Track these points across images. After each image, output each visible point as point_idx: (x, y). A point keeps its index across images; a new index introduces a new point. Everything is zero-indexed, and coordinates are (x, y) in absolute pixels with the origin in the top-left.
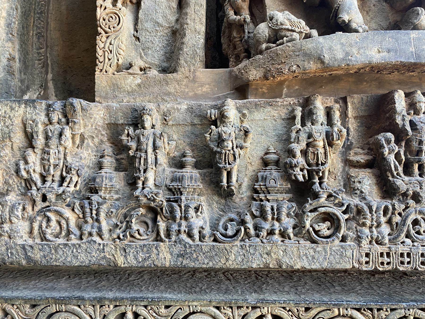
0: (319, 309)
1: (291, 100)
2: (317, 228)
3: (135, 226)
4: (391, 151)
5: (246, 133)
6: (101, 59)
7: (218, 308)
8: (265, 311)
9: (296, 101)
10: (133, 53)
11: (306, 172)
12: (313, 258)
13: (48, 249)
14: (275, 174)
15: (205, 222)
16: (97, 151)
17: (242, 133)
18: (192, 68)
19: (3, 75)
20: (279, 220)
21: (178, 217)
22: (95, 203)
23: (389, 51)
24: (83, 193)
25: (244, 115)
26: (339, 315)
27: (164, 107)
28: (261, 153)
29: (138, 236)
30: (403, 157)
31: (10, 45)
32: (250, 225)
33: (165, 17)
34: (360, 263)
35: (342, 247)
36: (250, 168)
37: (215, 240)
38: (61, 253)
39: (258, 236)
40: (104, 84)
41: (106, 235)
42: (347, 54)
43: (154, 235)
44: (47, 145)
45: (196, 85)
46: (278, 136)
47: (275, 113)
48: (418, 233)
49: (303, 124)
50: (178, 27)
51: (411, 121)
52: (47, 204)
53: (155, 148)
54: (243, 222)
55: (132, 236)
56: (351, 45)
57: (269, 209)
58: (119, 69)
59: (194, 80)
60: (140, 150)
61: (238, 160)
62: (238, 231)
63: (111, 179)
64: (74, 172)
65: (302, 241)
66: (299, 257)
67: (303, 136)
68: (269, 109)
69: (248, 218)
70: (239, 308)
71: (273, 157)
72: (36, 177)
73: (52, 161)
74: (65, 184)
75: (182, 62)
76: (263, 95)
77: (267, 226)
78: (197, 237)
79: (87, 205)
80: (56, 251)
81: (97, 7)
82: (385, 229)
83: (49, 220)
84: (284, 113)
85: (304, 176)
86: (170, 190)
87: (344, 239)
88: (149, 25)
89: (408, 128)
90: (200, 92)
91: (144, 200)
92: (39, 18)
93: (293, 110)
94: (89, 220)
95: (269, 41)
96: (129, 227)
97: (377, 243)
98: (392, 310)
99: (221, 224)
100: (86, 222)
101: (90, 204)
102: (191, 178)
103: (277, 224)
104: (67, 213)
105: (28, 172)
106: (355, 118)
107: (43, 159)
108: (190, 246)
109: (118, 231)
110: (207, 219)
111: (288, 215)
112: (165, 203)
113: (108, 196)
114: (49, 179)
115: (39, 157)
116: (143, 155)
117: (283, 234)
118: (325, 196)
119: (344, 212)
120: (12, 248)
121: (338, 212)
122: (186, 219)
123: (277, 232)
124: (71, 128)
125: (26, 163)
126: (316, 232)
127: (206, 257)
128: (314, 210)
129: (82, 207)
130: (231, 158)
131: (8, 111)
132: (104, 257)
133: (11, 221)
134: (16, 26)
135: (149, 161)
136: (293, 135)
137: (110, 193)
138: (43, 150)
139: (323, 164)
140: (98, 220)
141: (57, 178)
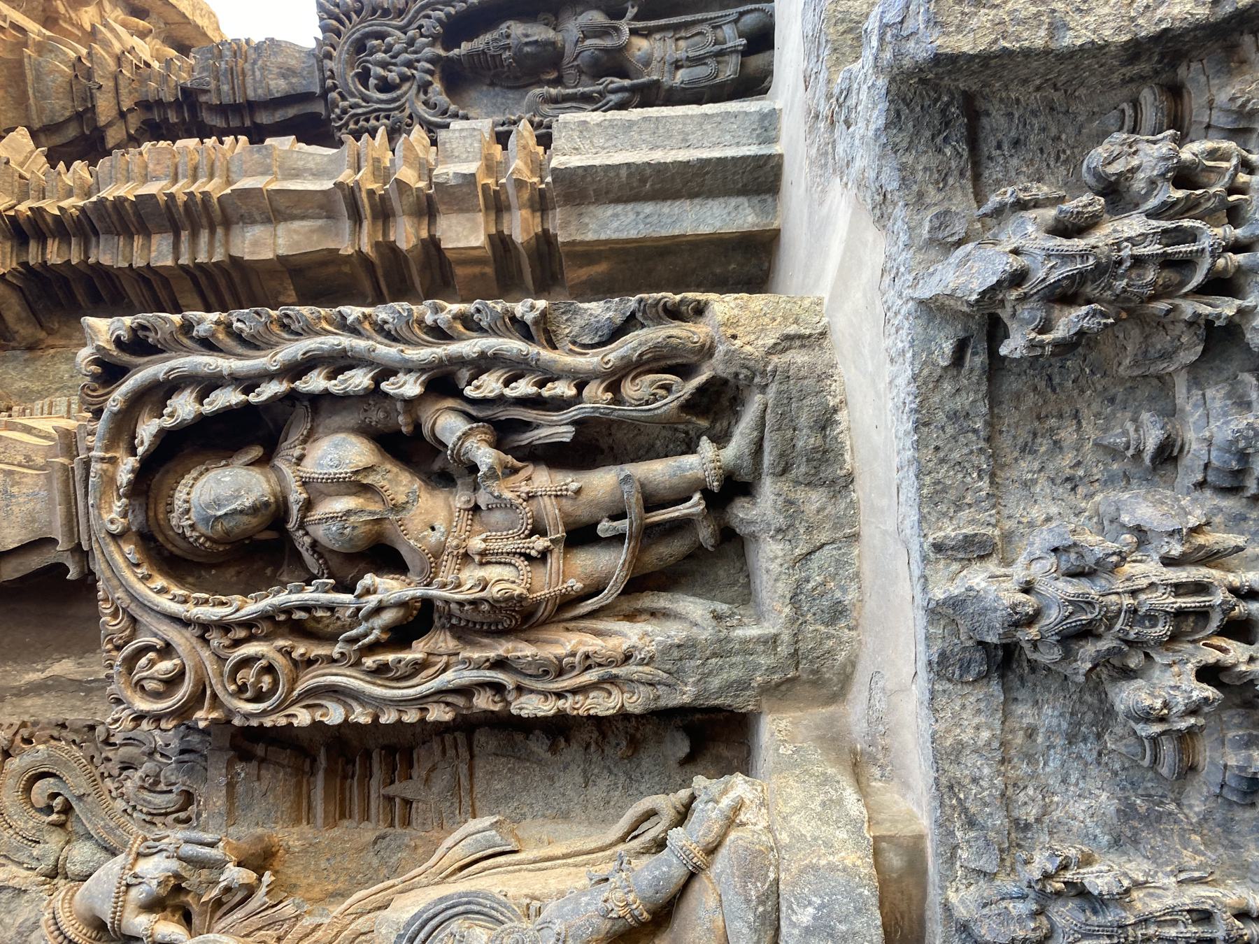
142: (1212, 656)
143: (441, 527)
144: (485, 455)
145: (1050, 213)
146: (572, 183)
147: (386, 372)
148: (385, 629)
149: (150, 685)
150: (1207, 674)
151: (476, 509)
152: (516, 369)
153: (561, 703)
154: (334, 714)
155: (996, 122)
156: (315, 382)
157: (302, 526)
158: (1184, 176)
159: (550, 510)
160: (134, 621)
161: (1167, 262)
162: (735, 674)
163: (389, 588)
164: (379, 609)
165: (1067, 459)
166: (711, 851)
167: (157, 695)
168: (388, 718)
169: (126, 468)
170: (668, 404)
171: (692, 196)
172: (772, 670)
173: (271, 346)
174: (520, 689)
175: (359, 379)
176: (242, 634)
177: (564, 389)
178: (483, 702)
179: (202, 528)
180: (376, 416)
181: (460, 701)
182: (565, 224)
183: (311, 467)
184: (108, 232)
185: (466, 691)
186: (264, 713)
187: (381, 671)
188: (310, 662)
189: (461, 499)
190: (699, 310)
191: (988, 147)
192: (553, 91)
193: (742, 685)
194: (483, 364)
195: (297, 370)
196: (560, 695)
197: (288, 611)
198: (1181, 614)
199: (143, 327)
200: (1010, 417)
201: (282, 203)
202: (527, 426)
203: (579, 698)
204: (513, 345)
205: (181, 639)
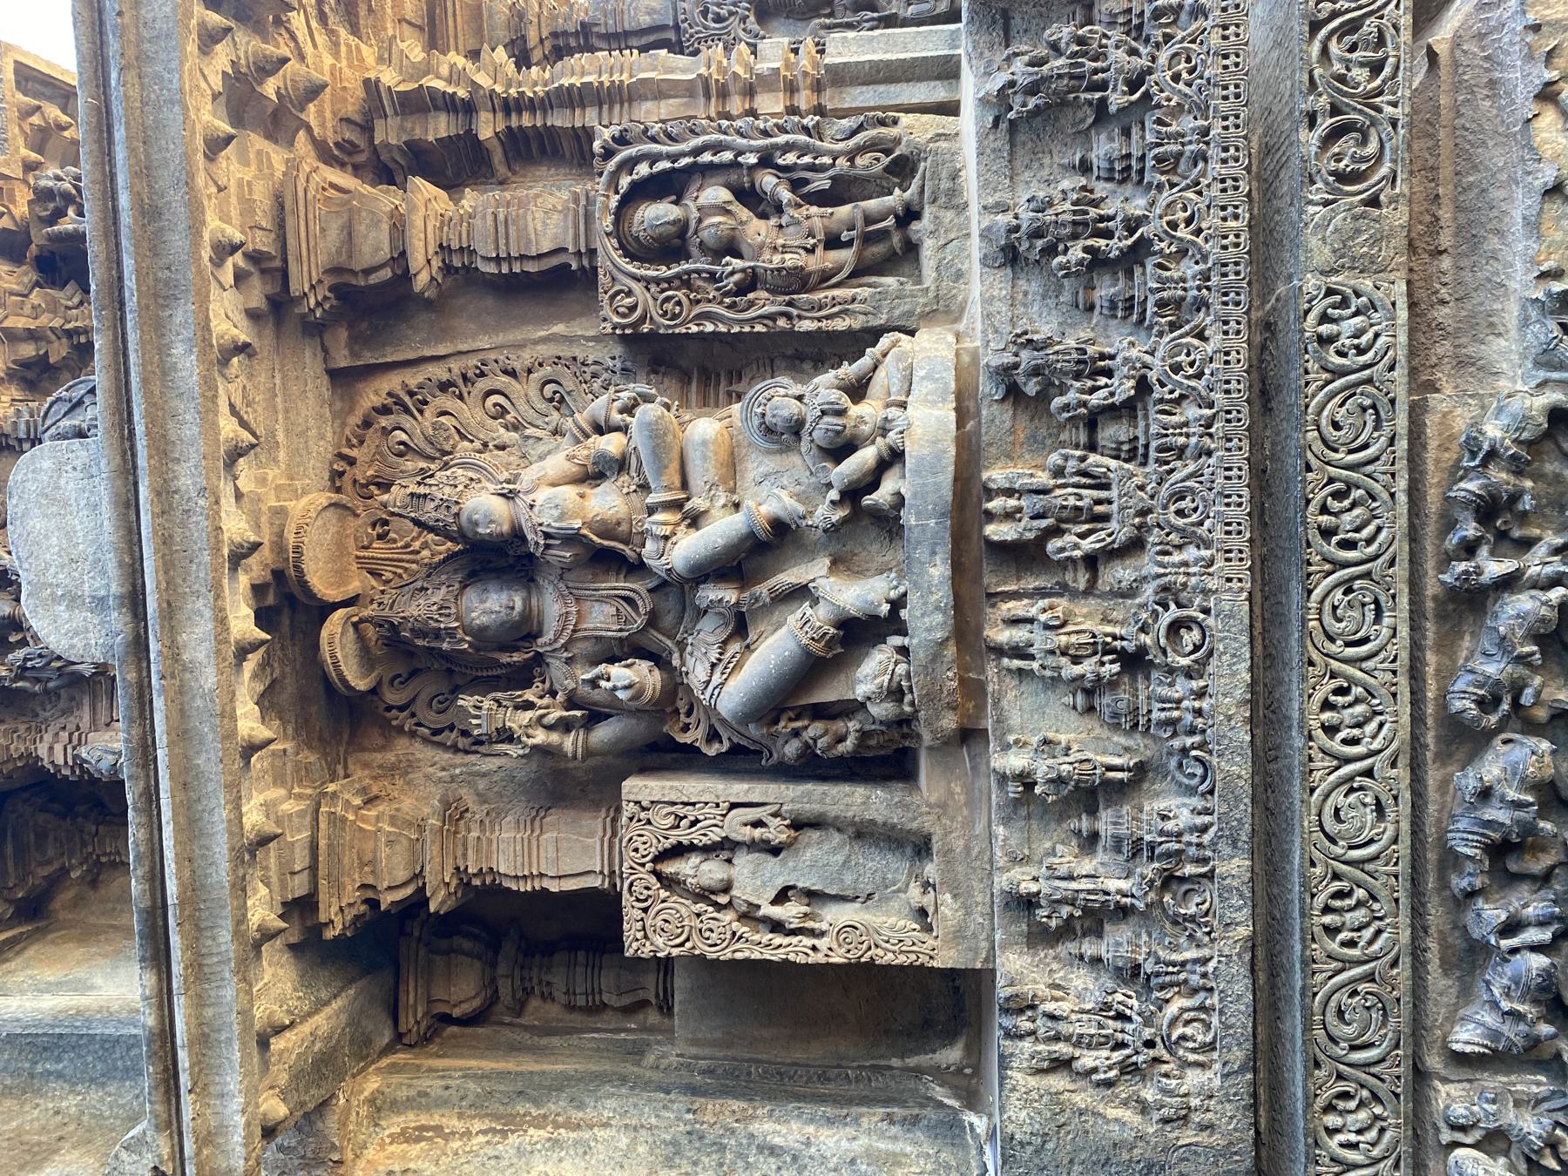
0: (1311, 648)
1: (991, 671)
2: (1190, 648)
3: (1192, 910)
4: (1076, 546)
5: (1046, 742)
6: (913, 957)
7: (1312, 790)
8: (1315, 724)
9: (993, 664)
10: (895, 904)
11: (1106, 658)
12: (1234, 656)
13: (1228, 1039)
14: (1106, 700)
15: (1184, 805)
16: (1072, 965)
17: (1046, 748)
18: (924, 809)
19: (919, 1134)
20: (1179, 701)
21: (1177, 846)
22: (1157, 968)
23: (934, 553)
24: (1138, 988)
25: (1016, 742)
26: (1320, 620)
27: (1000, 859)
28: (1073, 715)
29: (1207, 905)
30: (1087, 526)
31: (865, 1120)
32: (1189, 741)
33: (834, 851)
34: (1241, 590)
35: (1217, 616)
36: (1098, 731)
37: (1211, 792)
38: (1233, 1020)
39: (1203, 731)
40: (952, 953)
41: (1206, 952)
42: (937, 608)
43: (1205, 881)
44: (1068, 1039)
45: (950, 802)
46: (1046, 689)
47: (1011, 695)
48: (1195, 510)
49: (1032, 657)
50: (851, 830)
51: (1032, 518)
52: (1158, 1040)
53: (1071, 878)
54: (1184, 751)
55: (1206, 914)
56: (925, 604)
57: (1163, 715)
58: (928, 929)
59: (943, 806)
60: (1075, 899)
61: (1090, 755)
62: (1197, 759)
63: (1118, 944)
64: (1110, 998)
65: (1210, 669)
66: (1233, 675)
67: (1050, 661)
68: (1004, 703)
69: (1176, 743)
70: (1311, 759)
71: (1080, 699)
72: (1117, 1056)
73: (1093, 1031)
74: (1128, 1012)
75: (915, 825)
76: (981, 707)
77: (1189, 718)
78: (1207, 819)
79: (1160, 980)
80: (1231, 1027)
81: (828, 964)
82: (1191, 553)
83: (1183, 1038)
84: (1010, 682)
85: (1112, 662)
86: (1134, 855)
87: (1206, 611)
88: (848, 878)
89: (1044, 523)
90: (962, 797)
91: (1152, 896)
92: (791, 1078)
93: (1009, 670)
94: (1182, 976)
95: (901, 701)
96: (1192, 919)
97: (1211, 565)
98: (1309, 545)
99: (1186, 781)
100: (1186, 981)
101: (1158, 975)
102: (1115, 824)
103: (1185, 704)
104: (1172, 1009)
105: (1110, 1068)
106: (1019, 580)
107: (1089, 1047)
108: (1220, 829)
109: (1199, 934)
110: (1180, 800)
111: (1171, 685)
112: (1156, 865)
113: (1144, 949)
114: (1119, 1036)
115: (1085, 1052)
116: (1082, 896)
117: (1201, 694)
118: (1142, 636)
119: (1166, 607)
120: (1227, 1094)
121: (1166, 618)
122: (1180, 834)
123: (1197, 704)
124: (1043, 1001)
125: (1095, 1070)
126: (1197, 648)
127: (1237, 807)
128: (1164, 652)
129: (1162, 988)
130: (1086, 766)
131: (1017, 1095)
132: (1239, 955)
133: (1185, 1095)
134: (830, 1111)
135: (1091, 886)
136: (1048, 673)
137: (1139, 946)
138: (1075, 1046)
139: (1094, 636)
140: (1183, 964)
141: (1119, 1025)
142: (1090, 242)
143: (763, 233)
144: (786, 195)
145: (1026, 58)
146: (836, 73)
147: (740, 153)
148: (736, 284)
149: (621, 310)
150: (1086, 249)
151: (781, 226)
152: (804, 150)
154: (709, 328)
155: (1017, 22)
156: (707, 157)
158: (1081, 41)
159: (817, 223)
160: (613, 279)
161: (1072, 77)
162: (907, 308)
163: (737, 263)
164: (732, 273)
165: (1046, 171)
166: (885, 355)
167: (624, 316)
168: (736, 329)
169: (614, 201)
170: (878, 168)
171: (908, 81)
172: (925, 305)
173: (685, 140)
174: (800, 317)
175: (727, 156)
177: (827, 160)
180: (734, 177)
182: (832, 99)
183: (701, 201)
184: (561, 106)
185: (772, 317)
186: (676, 326)
187: (731, 306)
188: (698, 302)
189: (773, 221)
190: (895, 122)
191: (1013, 33)
192: (827, 21)
193: (910, 314)
194: (787, 148)
195: (697, 152)
196: (819, 320)
197: (688, 273)
198: (1074, 223)
200: (1020, 151)
202: (806, 182)
204: (803, 138)
205: (637, 288)
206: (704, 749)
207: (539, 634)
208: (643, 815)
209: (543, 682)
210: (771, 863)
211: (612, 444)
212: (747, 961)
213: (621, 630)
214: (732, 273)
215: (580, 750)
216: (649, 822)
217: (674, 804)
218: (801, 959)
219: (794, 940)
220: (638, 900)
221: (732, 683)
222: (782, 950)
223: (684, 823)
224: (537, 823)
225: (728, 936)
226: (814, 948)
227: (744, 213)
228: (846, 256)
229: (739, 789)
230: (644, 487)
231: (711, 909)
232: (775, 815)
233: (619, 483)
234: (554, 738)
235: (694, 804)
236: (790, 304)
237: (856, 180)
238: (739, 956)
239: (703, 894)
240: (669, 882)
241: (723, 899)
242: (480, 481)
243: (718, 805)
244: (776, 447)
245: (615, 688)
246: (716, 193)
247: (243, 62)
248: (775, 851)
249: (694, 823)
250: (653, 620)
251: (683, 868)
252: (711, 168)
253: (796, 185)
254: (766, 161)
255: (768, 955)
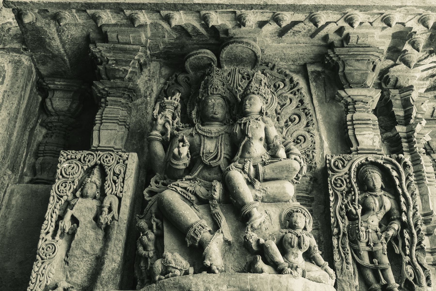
143: (373, 223)
144: (391, 233)
147: (407, 214)
148: (351, 210)
149: (337, 163)
153: (336, 247)
154: (332, 199)
156: (403, 199)
157: (371, 195)
163: (359, 211)
164: (355, 209)
168: (332, 210)
174: (338, 239)
176: (348, 181)
178: (336, 231)
179: (369, 175)
181: (335, 225)
183: (384, 197)
185: (338, 226)
187: (341, 209)
188: (342, 194)
189: (378, 229)
194: (411, 235)
196: (338, 247)
197: (354, 190)
199: (410, 167)
201: (426, 197)
202: (398, 245)
203: (337, 252)
205: (346, 170)
206: (146, 190)
207: (203, 125)
208: (121, 161)
209: (183, 127)
210: (91, 216)
211: (282, 153)
212: (48, 202)
213: (203, 153)
214: (355, 209)
215: (153, 137)
216: (118, 163)
217: (125, 173)
218: (44, 226)
219: (53, 224)
220: (85, 157)
221: (177, 195)
222: (50, 218)
223: (115, 178)
224: (123, 123)
225: (61, 194)
226: (48, 233)
227: (381, 215)
228: (366, 261)
229: (127, 202)
230: (264, 164)
231: (75, 187)
232: (113, 218)
233: (266, 154)
234: (160, 127)
235: (123, 182)
236: (344, 234)
237: (401, 266)
238: (51, 198)
239: (82, 185)
240: (89, 172)
241: (78, 194)
242: (266, 103)
243: (121, 192)
244: (283, 219)
245: (179, 147)
246: (388, 203)
247: (416, 36)
248: (96, 219)
249: (115, 182)
250: (208, 167)
251: (96, 177)
252: (398, 202)
253: (395, 238)
254: (405, 225)
255: (49, 211)
